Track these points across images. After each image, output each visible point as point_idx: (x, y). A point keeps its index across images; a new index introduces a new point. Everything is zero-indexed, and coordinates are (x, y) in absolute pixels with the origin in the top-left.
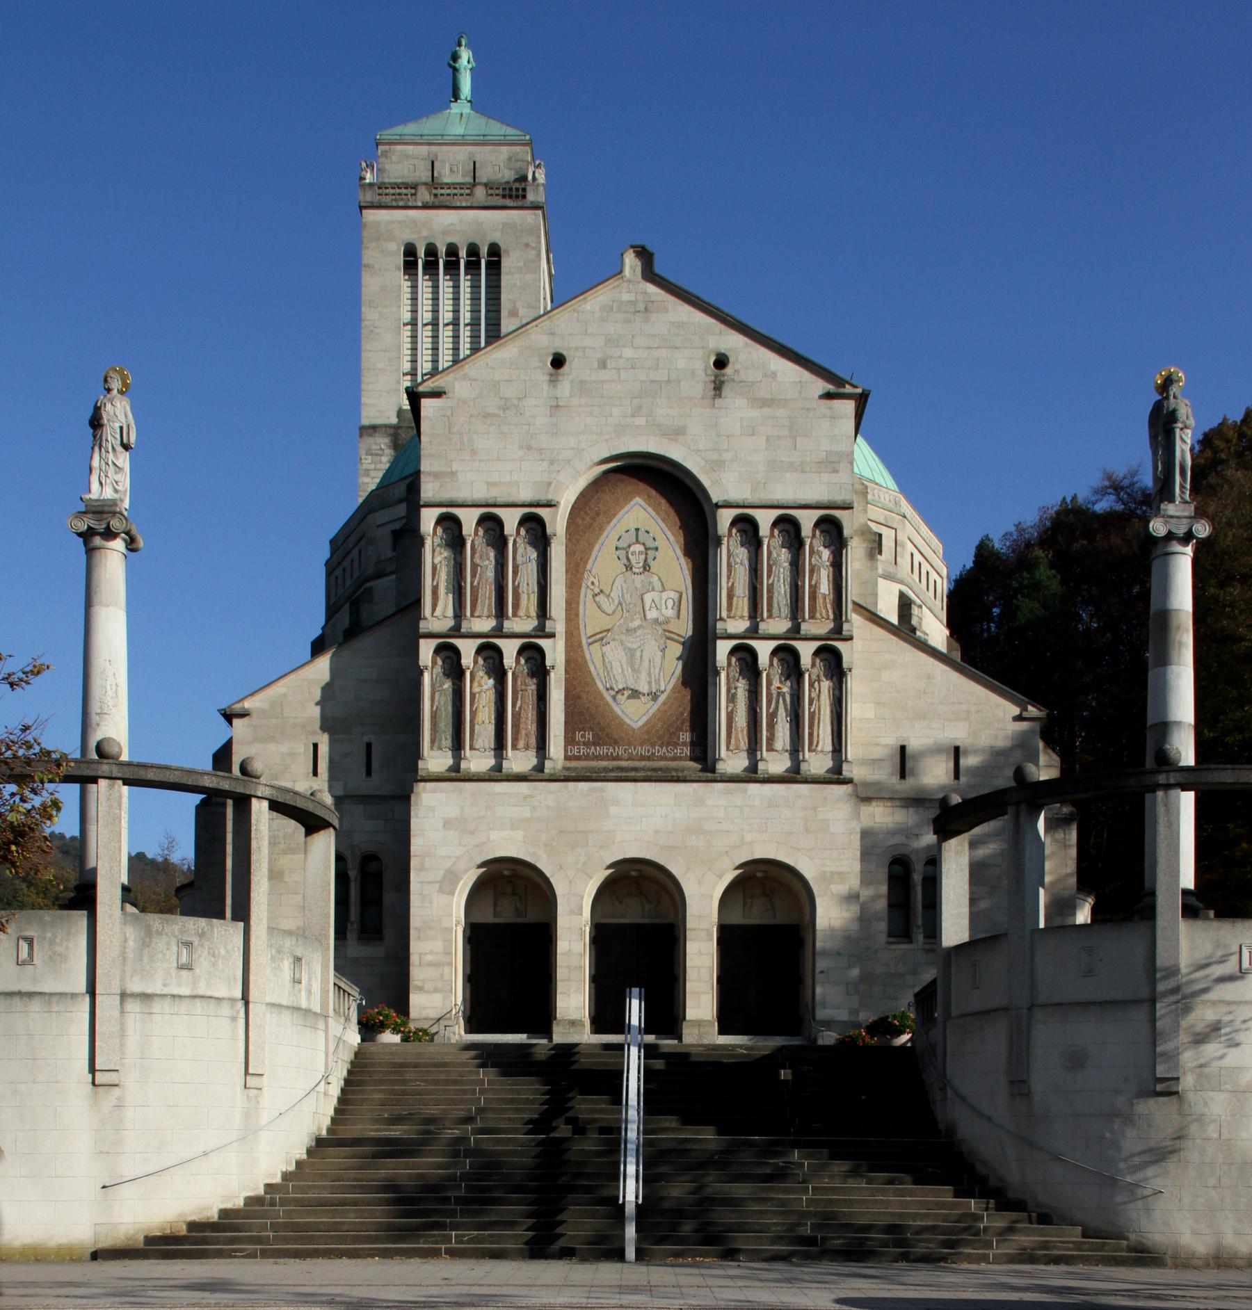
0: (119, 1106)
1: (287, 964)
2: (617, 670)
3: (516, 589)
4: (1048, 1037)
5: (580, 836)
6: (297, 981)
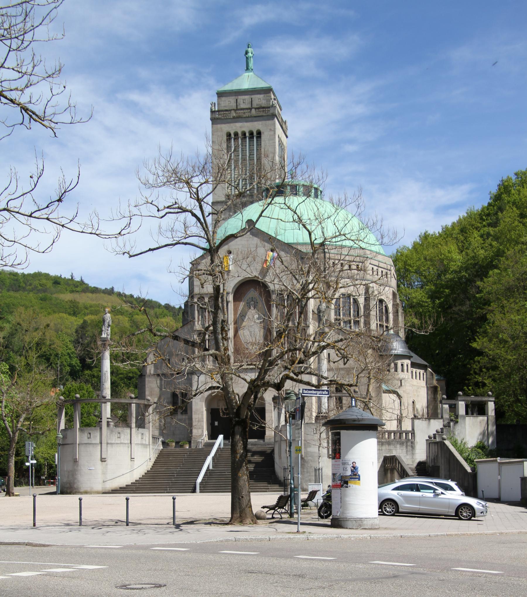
0: (107, 465)
1: (140, 435)
6: (142, 438)
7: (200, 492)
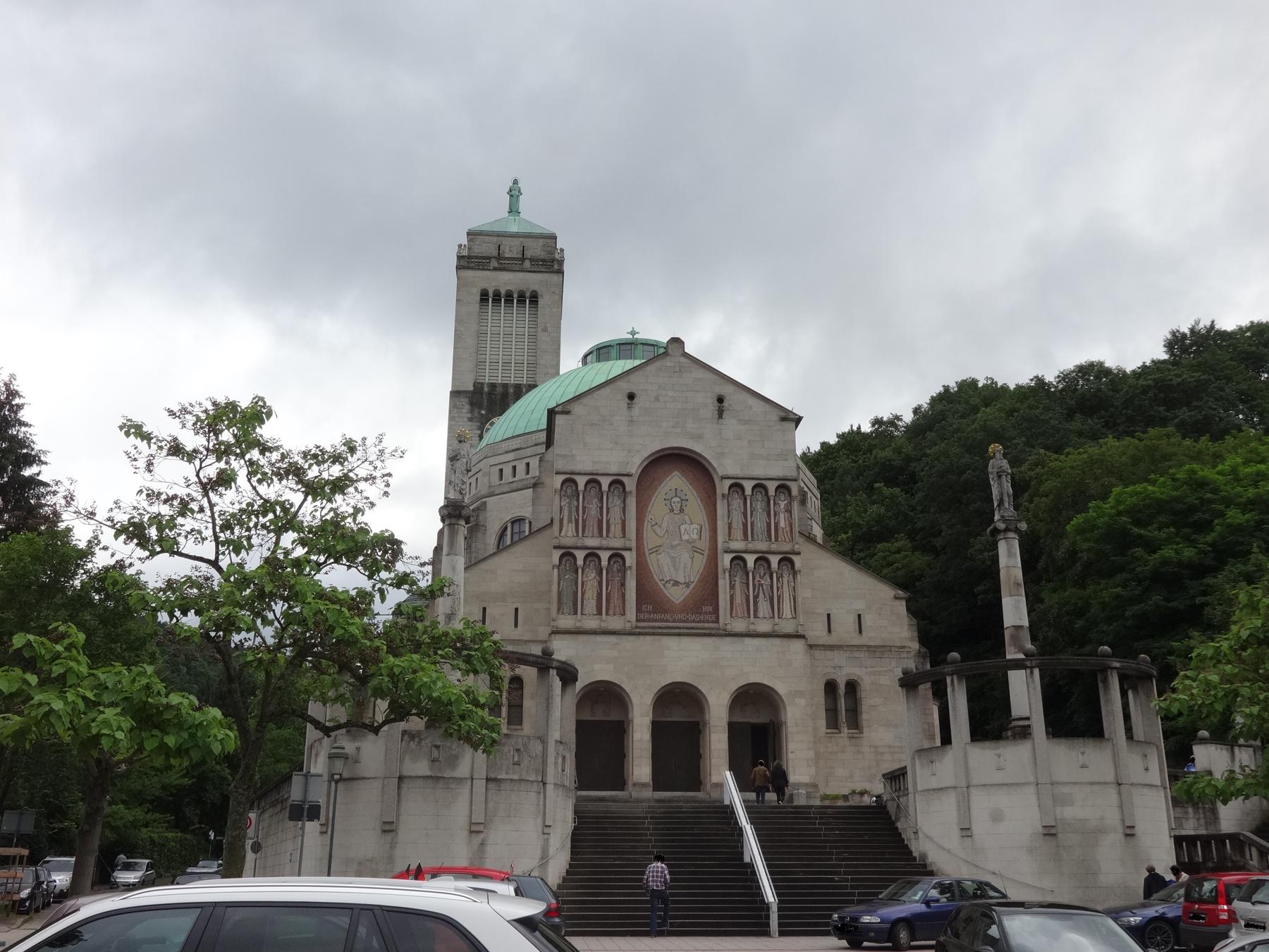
0: (482, 844)
2: (666, 569)
3: (608, 521)
4: (981, 803)
5: (642, 668)
7: (782, 934)
